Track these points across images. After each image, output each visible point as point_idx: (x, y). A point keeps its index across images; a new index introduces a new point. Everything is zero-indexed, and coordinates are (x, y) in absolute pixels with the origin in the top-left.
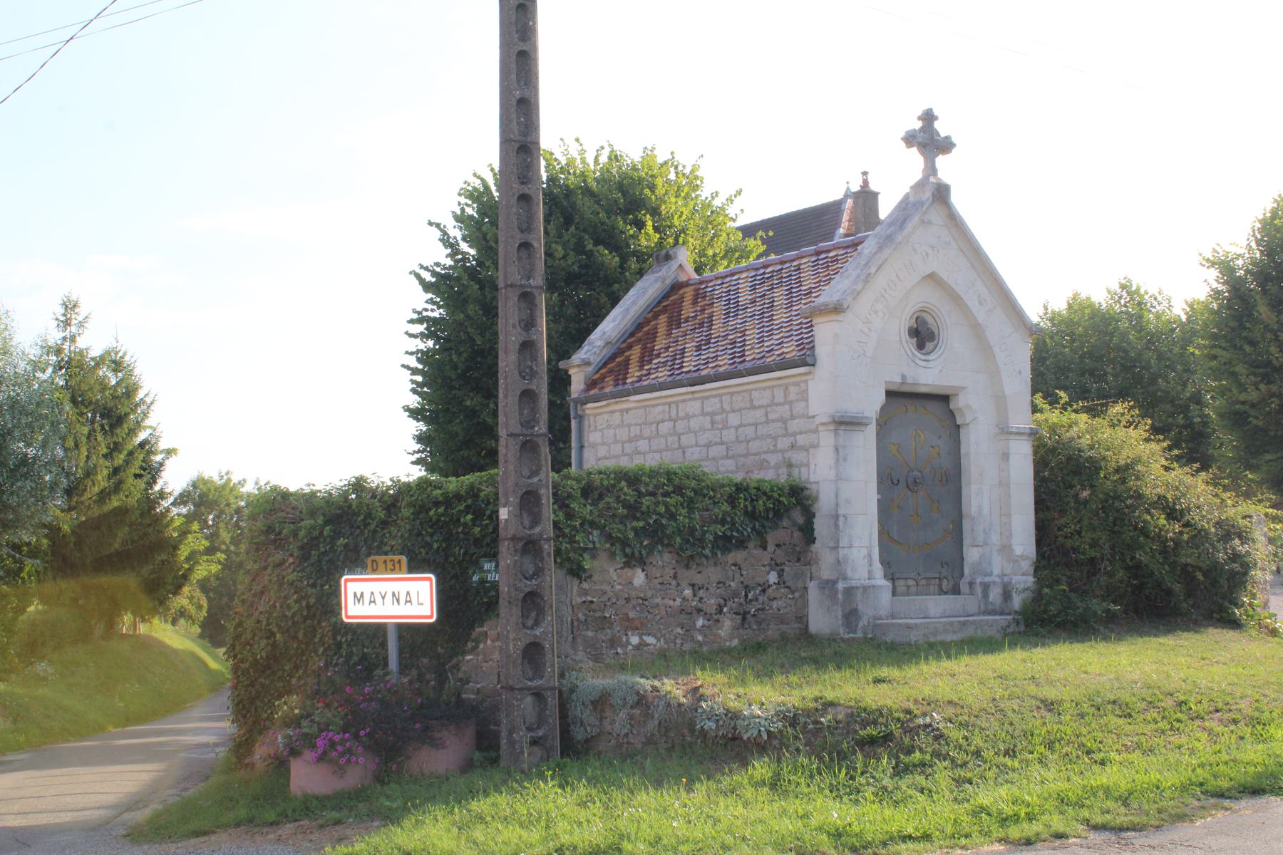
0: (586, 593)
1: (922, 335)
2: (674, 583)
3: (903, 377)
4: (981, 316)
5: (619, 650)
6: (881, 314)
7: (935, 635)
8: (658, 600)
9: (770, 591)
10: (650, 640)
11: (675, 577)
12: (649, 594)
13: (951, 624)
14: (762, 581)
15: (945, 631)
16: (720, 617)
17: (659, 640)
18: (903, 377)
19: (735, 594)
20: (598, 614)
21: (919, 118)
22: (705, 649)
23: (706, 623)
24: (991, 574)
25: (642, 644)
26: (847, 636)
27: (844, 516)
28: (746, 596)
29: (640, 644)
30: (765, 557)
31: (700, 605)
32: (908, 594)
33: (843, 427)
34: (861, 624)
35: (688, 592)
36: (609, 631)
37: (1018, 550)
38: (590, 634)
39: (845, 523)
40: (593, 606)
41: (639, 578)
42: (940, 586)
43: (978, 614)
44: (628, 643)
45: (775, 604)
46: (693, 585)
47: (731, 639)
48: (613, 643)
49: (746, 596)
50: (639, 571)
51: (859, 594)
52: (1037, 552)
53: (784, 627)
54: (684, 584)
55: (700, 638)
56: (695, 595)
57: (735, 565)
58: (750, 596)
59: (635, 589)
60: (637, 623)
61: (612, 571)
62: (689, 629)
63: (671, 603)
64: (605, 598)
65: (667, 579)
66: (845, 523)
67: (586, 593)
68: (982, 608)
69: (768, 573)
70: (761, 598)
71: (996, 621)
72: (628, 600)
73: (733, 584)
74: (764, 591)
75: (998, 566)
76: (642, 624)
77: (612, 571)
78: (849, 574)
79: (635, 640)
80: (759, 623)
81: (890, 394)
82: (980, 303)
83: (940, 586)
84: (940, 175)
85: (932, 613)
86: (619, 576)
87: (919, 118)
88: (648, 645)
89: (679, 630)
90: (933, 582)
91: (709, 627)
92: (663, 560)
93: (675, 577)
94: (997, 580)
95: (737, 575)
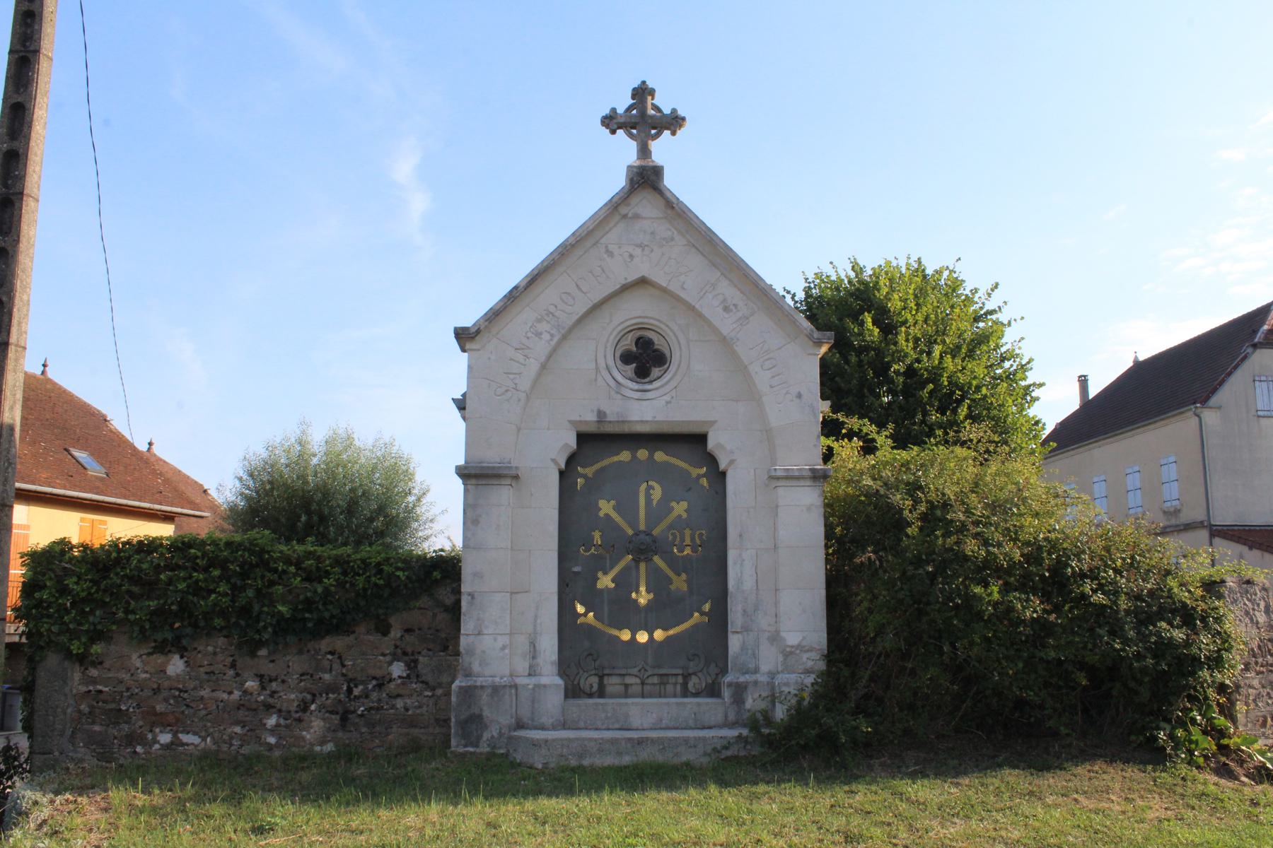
0: (94, 681)
1: (645, 358)
2: (231, 672)
3: (601, 414)
4: (726, 325)
5: (139, 749)
6: (546, 337)
7: (581, 756)
8: (205, 693)
9: (392, 685)
10: (185, 738)
11: (233, 666)
12: (191, 685)
13: (614, 741)
14: (378, 673)
15: (601, 751)
16: (306, 716)
17: (204, 739)
18: (601, 414)
19: (331, 688)
20: (113, 706)
21: (674, 111)
22: (277, 753)
23: (282, 721)
24: (756, 671)
25: (176, 743)
26: (461, 750)
27: (471, 595)
28: (350, 691)
29: (172, 743)
30: (387, 644)
31: (271, 701)
32: (626, 696)
33: (473, 481)
34: (486, 736)
35: (251, 684)
36: (126, 727)
37: (792, 639)
38: (97, 728)
39: (471, 603)
40: (102, 697)
41: (176, 666)
42: (685, 685)
43: (720, 727)
44: (155, 741)
45: (399, 703)
46: (261, 677)
47: (323, 742)
48: (131, 739)
49: (350, 691)
50: (177, 657)
51: (485, 697)
52: (830, 640)
53: (416, 731)
54: (246, 675)
55: (272, 740)
56: (263, 688)
57: (332, 653)
58: (356, 692)
59: (169, 678)
60: (171, 719)
61: (134, 656)
62: (254, 731)
63: (225, 696)
64: (121, 688)
65: (218, 667)
66: (471, 603)
67: (94, 681)
68: (732, 717)
69: (390, 663)
70: (374, 696)
71: (704, 739)
72: (156, 691)
73: (327, 676)
74: (380, 686)
75: (768, 660)
76: (178, 720)
77: (134, 656)
78: (476, 668)
79: (165, 738)
80: (371, 725)
81: (582, 438)
82: (726, 309)
83: (685, 685)
84: (654, 157)
85: (636, 722)
86: (145, 663)
87: (674, 111)
88: (183, 744)
89: (238, 729)
90: (672, 680)
91: (287, 726)
92: (214, 649)
93: (233, 666)
94: (762, 678)
95: (336, 666)
